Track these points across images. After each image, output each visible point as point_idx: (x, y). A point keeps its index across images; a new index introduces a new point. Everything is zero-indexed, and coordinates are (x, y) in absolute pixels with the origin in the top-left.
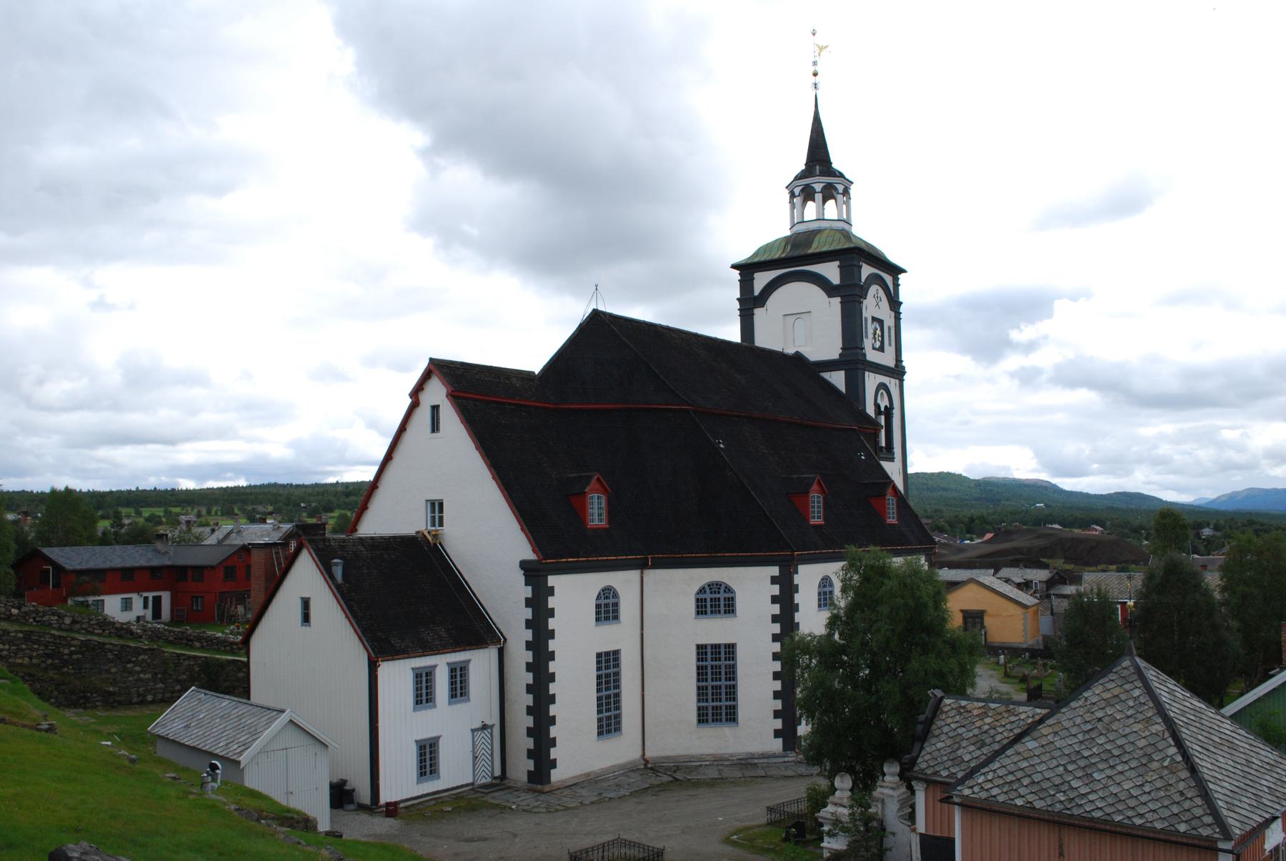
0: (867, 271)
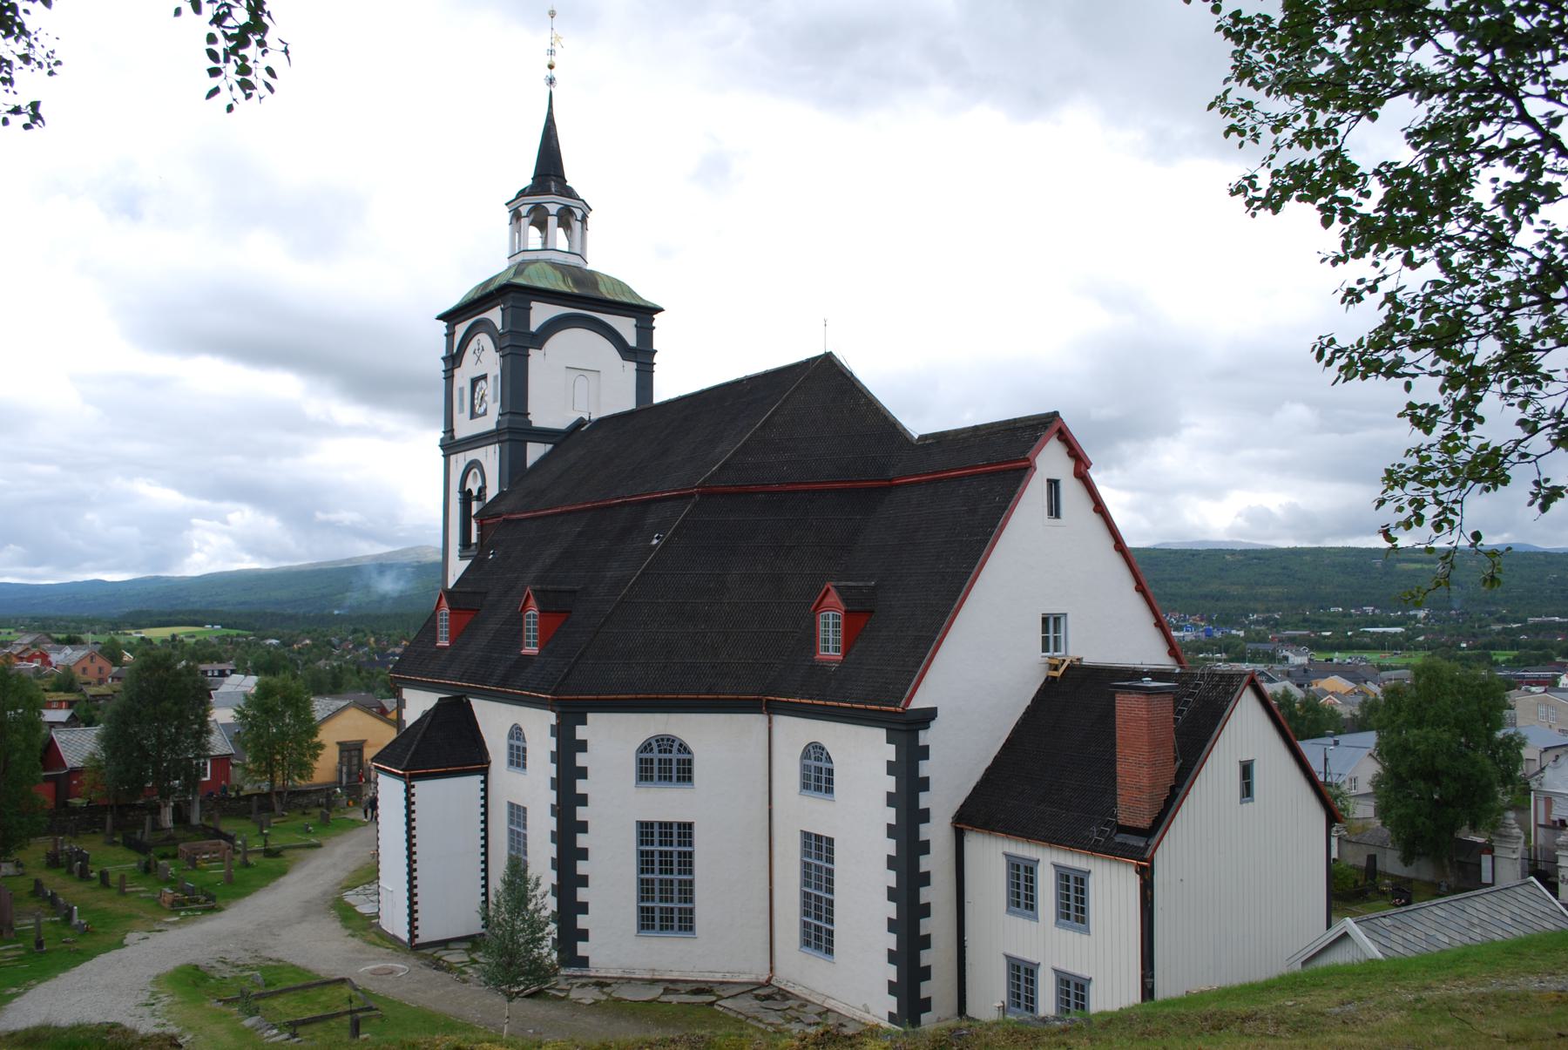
0: (541, 313)
